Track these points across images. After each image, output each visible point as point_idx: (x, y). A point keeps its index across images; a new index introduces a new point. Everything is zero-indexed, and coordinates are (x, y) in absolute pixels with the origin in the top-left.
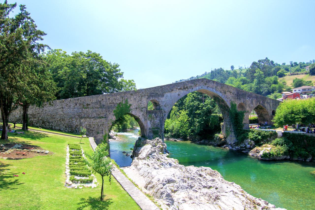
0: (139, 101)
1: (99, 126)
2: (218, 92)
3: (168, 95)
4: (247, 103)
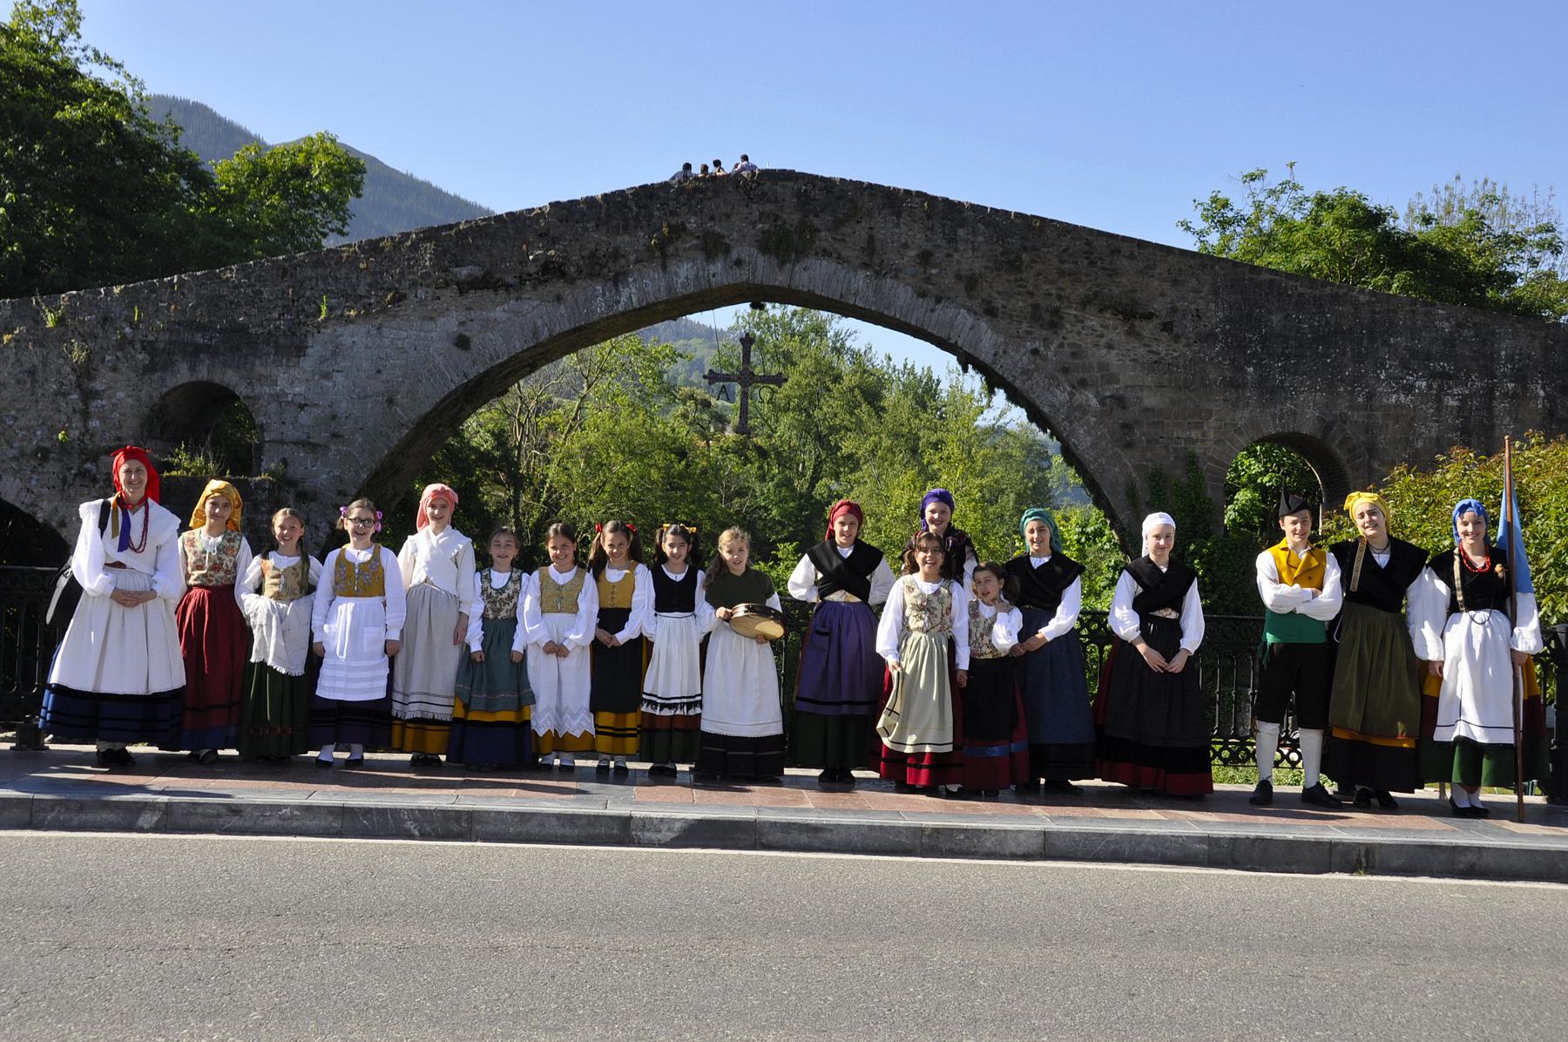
0: (64, 395)
2: (944, 312)
3: (347, 340)
4: (1382, 441)
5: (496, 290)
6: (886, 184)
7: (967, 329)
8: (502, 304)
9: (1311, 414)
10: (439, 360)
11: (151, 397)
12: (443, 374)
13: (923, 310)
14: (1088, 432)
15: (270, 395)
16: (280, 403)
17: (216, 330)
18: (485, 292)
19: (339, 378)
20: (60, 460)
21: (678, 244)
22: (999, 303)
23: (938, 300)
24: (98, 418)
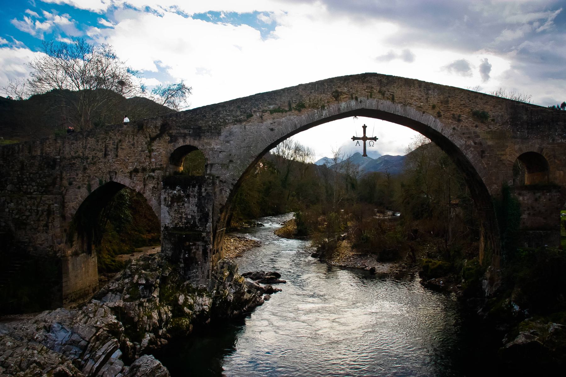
1: (40, 212)
5: (282, 112)
6: (405, 77)
7: (433, 122)
8: (284, 117)
9: (537, 146)
10: (264, 135)
11: (171, 151)
12: (266, 140)
13: (419, 116)
14: (471, 153)
15: (210, 149)
16: (213, 151)
17: (191, 128)
18: (279, 113)
19: (232, 142)
20: (142, 172)
21: (341, 97)
22: (442, 113)
23: (424, 113)
24: (154, 158)
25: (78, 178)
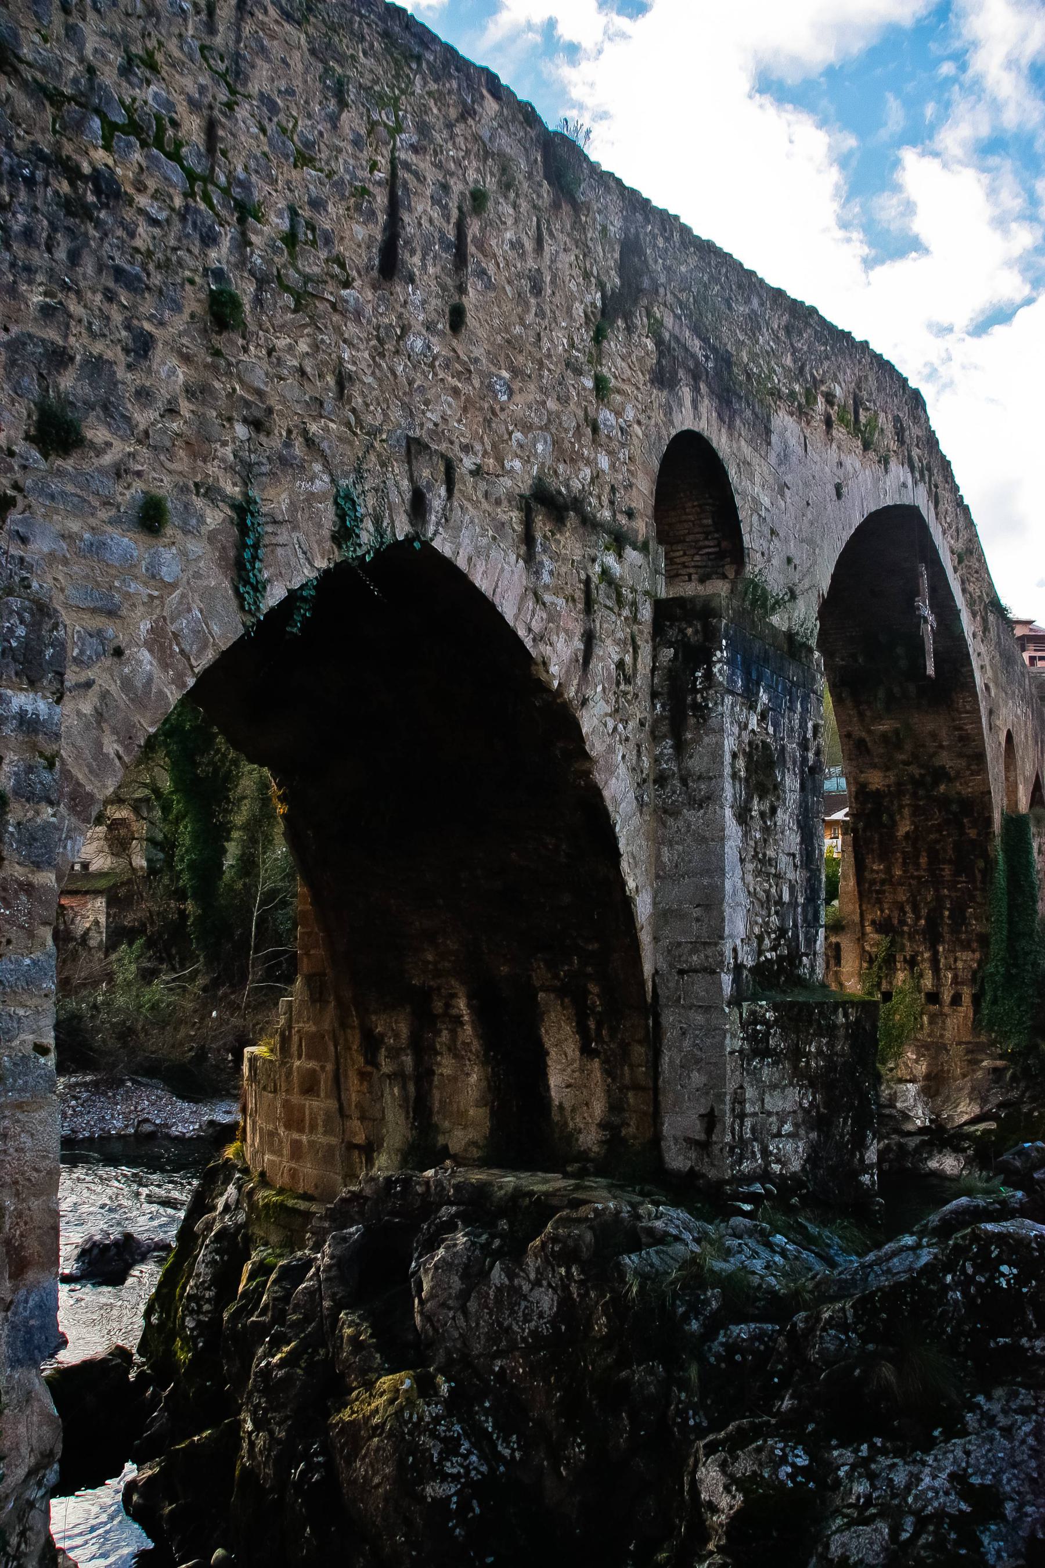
25: (144, 395)
